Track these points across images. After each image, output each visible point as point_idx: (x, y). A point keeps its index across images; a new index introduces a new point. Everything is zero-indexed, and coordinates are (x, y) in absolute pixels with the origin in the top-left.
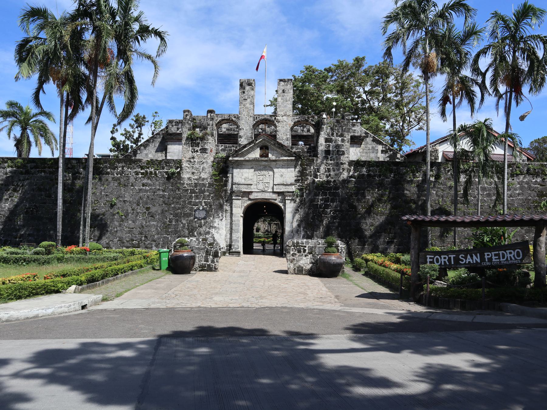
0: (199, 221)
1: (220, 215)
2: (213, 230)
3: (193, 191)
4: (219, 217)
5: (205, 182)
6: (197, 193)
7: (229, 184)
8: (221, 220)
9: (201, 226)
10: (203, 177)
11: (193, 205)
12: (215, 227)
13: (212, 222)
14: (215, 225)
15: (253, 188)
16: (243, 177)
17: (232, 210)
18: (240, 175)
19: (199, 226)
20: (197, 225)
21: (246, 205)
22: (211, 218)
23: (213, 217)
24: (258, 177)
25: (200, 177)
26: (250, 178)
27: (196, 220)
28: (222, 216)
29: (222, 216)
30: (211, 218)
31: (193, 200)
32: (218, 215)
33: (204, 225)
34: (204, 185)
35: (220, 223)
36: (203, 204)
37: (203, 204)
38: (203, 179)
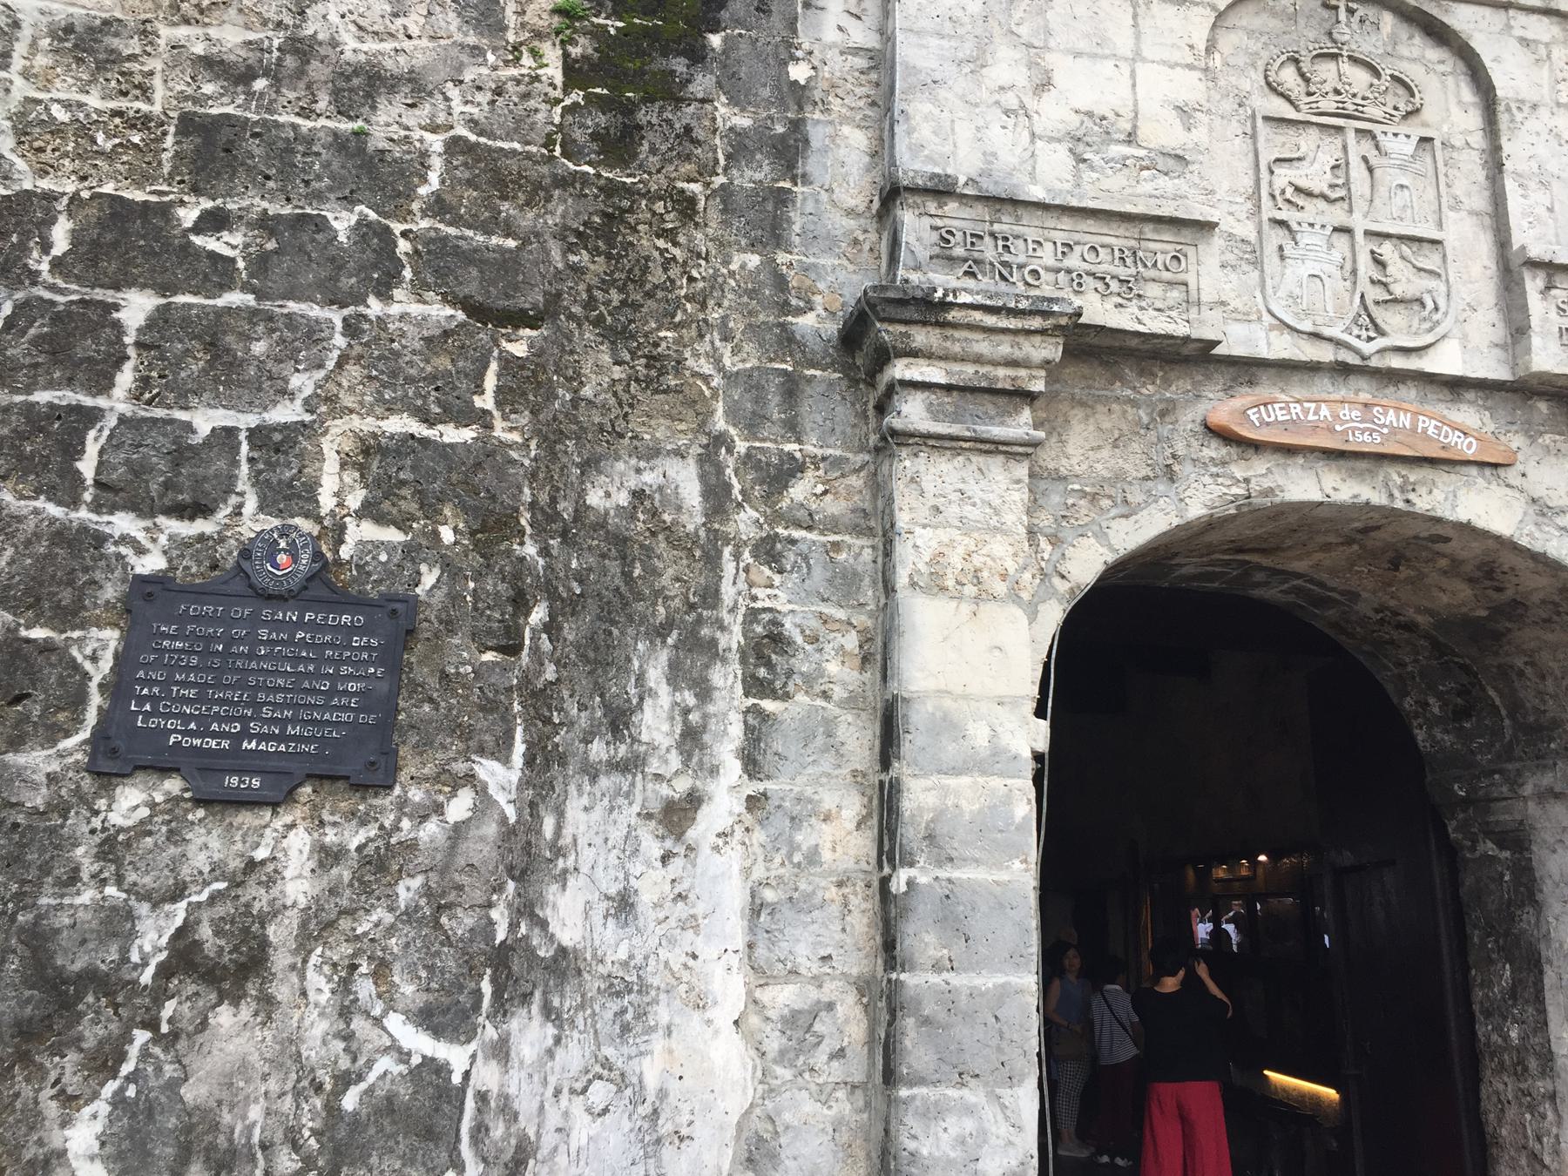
0: (207, 845)
1: (655, 724)
2: (529, 1033)
3: (125, 240)
4: (630, 766)
5: (387, 122)
6: (219, 272)
7: (841, 161)
8: (677, 816)
9: (231, 965)
10: (353, 48)
11: (111, 494)
12: (564, 965)
13: (528, 860)
14: (570, 916)
15: (1223, 301)
16: (1053, 113)
17: (879, 653)
18: (1007, 68)
19: (184, 956)
20: (153, 936)
21: (1086, 564)
22: (500, 777)
23: (544, 763)
24: (1273, 144)
25: (301, 48)
26: (1162, 132)
27: (129, 803)
28: (692, 739)
29: (692, 739)
30: (500, 777)
31: (118, 400)
32: (619, 721)
33: (317, 927)
34: (379, 175)
35: (651, 886)
36: (335, 486)
37: (335, 486)
38: (365, 85)
